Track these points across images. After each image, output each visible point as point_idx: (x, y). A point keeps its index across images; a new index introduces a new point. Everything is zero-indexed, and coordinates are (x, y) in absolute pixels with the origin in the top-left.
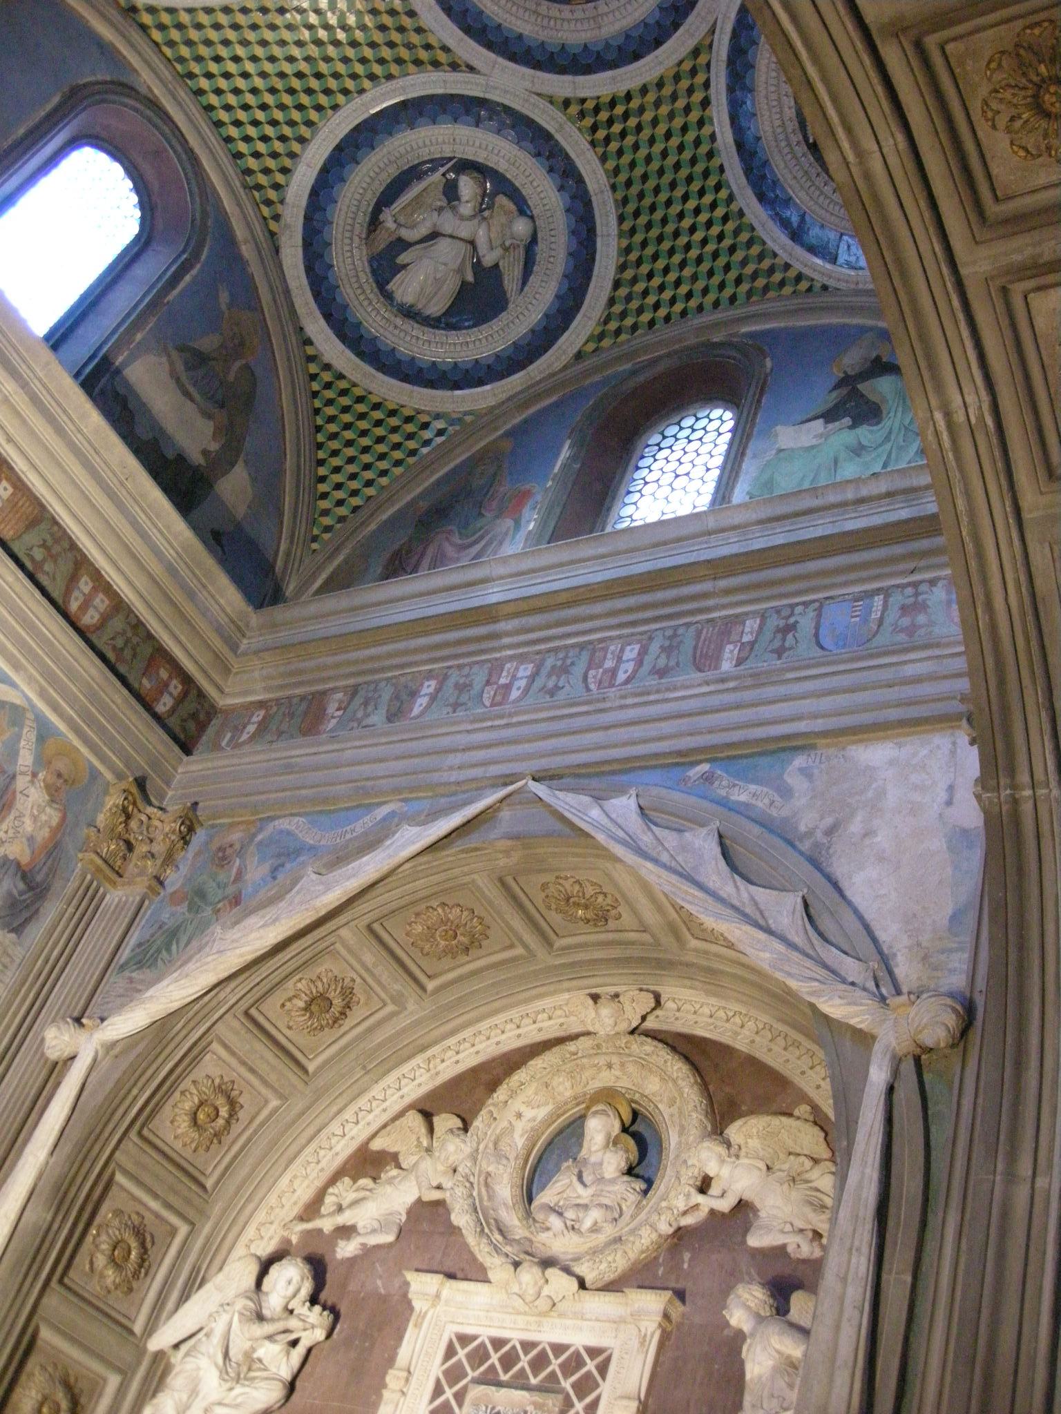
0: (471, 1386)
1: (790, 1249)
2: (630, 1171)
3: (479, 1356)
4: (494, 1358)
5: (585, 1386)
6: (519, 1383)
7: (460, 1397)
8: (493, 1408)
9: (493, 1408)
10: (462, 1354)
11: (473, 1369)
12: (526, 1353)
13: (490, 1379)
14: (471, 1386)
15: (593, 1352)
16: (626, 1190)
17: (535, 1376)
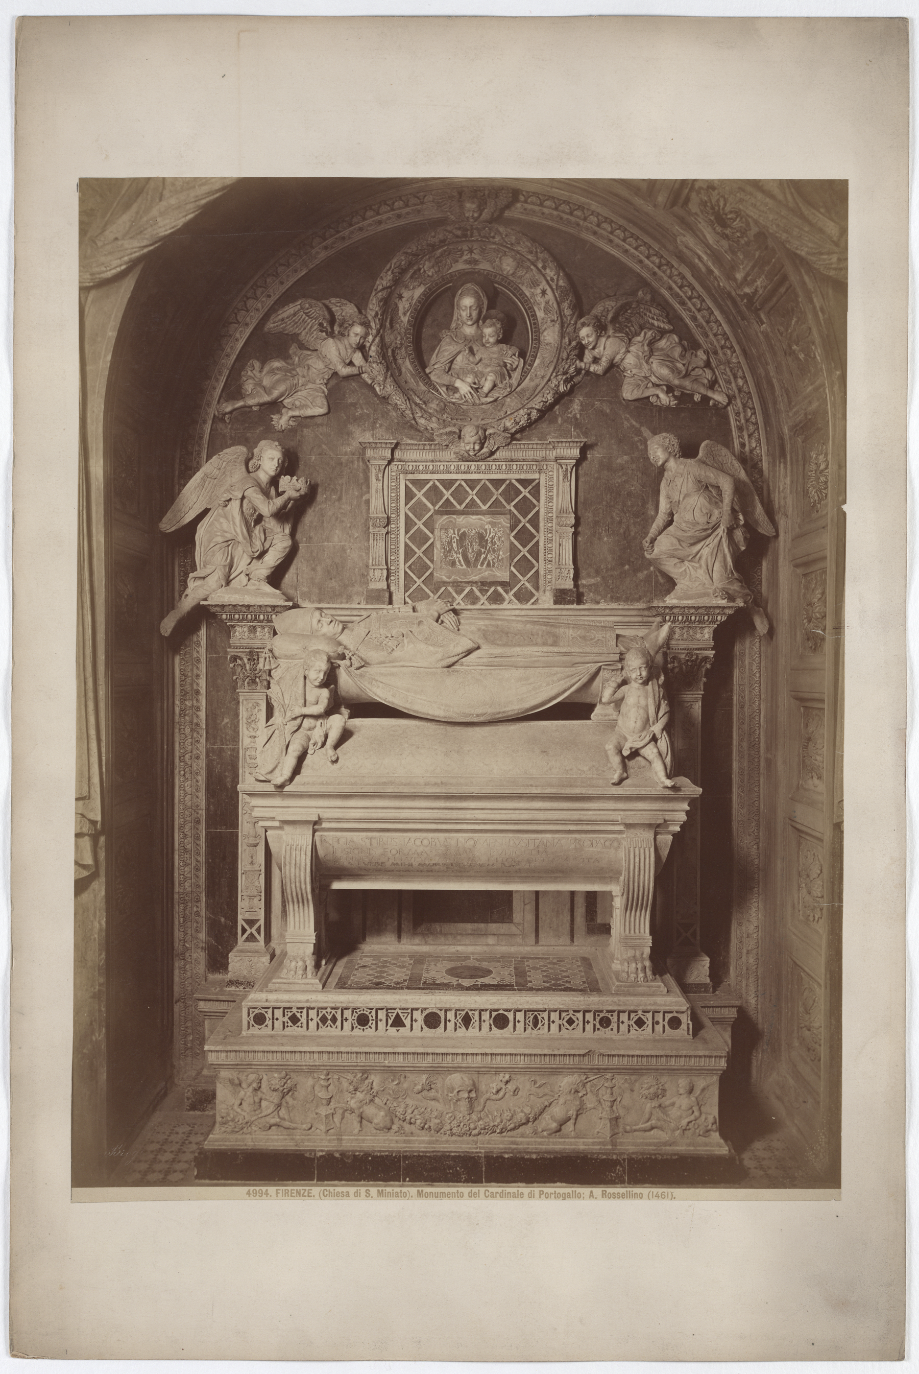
0: (435, 517)
1: (653, 400)
2: (505, 339)
3: (434, 493)
4: (447, 494)
5: (525, 507)
6: (471, 509)
7: (429, 524)
8: (459, 530)
9: (459, 530)
10: (419, 495)
11: (434, 505)
12: (472, 489)
13: (447, 510)
14: (435, 517)
15: (525, 483)
16: (511, 357)
17: (484, 504)
